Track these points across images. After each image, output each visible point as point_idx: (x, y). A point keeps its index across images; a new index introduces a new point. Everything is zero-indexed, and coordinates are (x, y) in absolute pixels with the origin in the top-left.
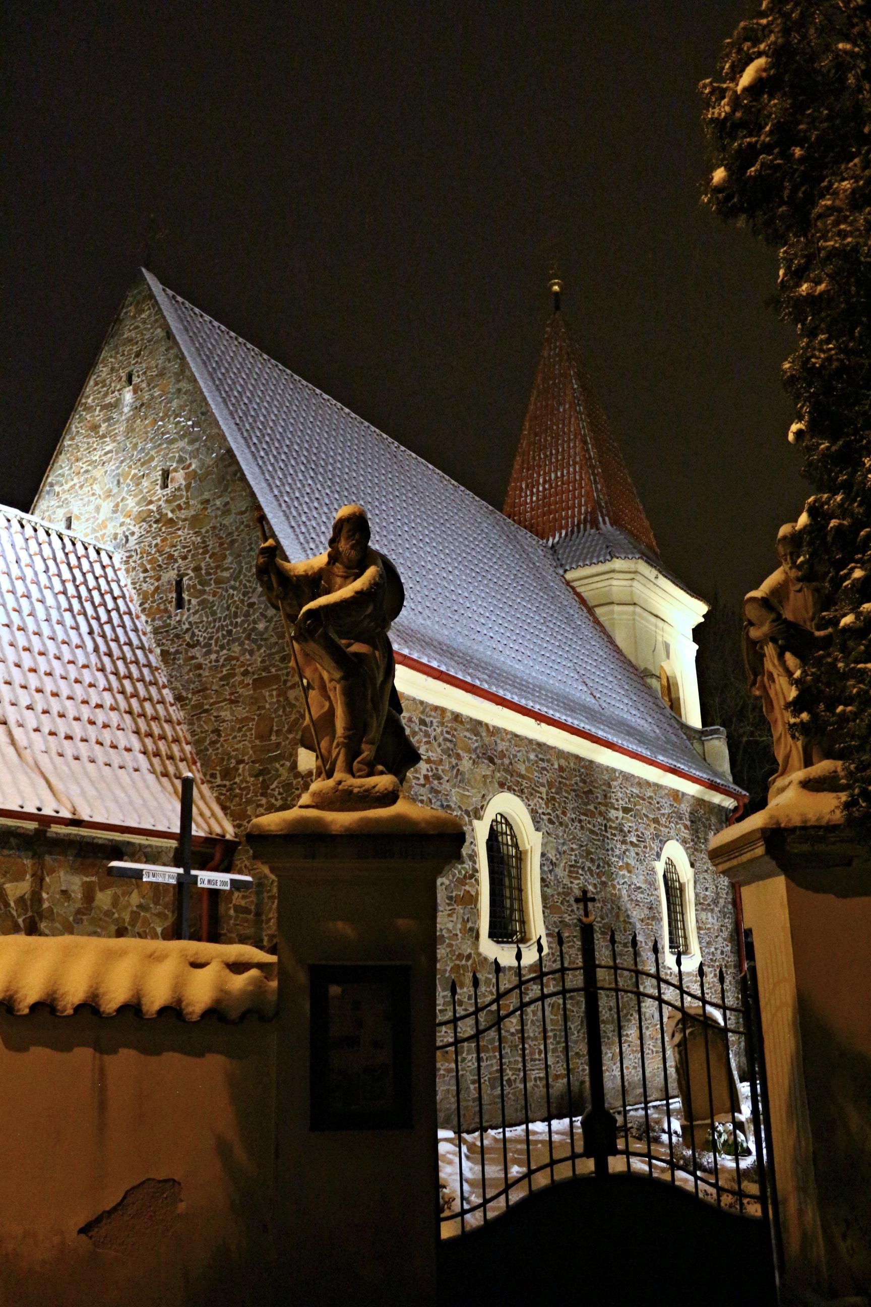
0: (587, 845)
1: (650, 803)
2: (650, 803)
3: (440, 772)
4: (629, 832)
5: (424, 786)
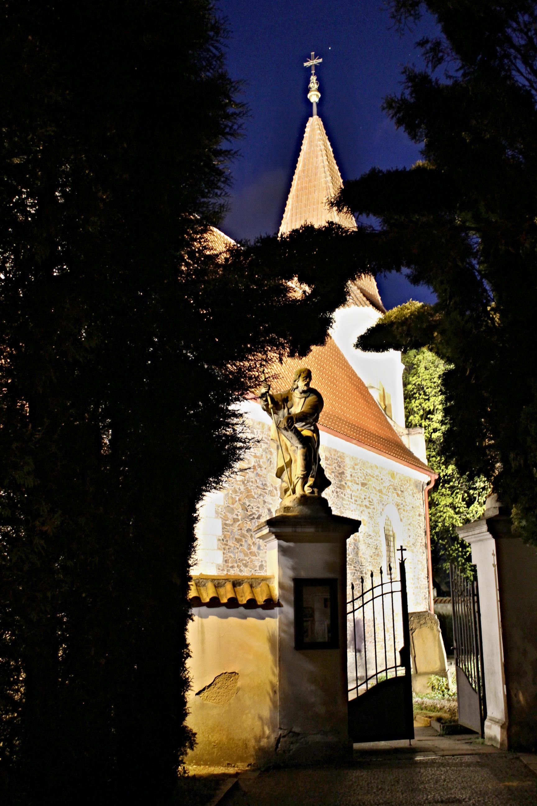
0: (340, 508)
1: (377, 479)
2: (377, 479)
3: (261, 463)
4: (365, 499)
5: (253, 472)
